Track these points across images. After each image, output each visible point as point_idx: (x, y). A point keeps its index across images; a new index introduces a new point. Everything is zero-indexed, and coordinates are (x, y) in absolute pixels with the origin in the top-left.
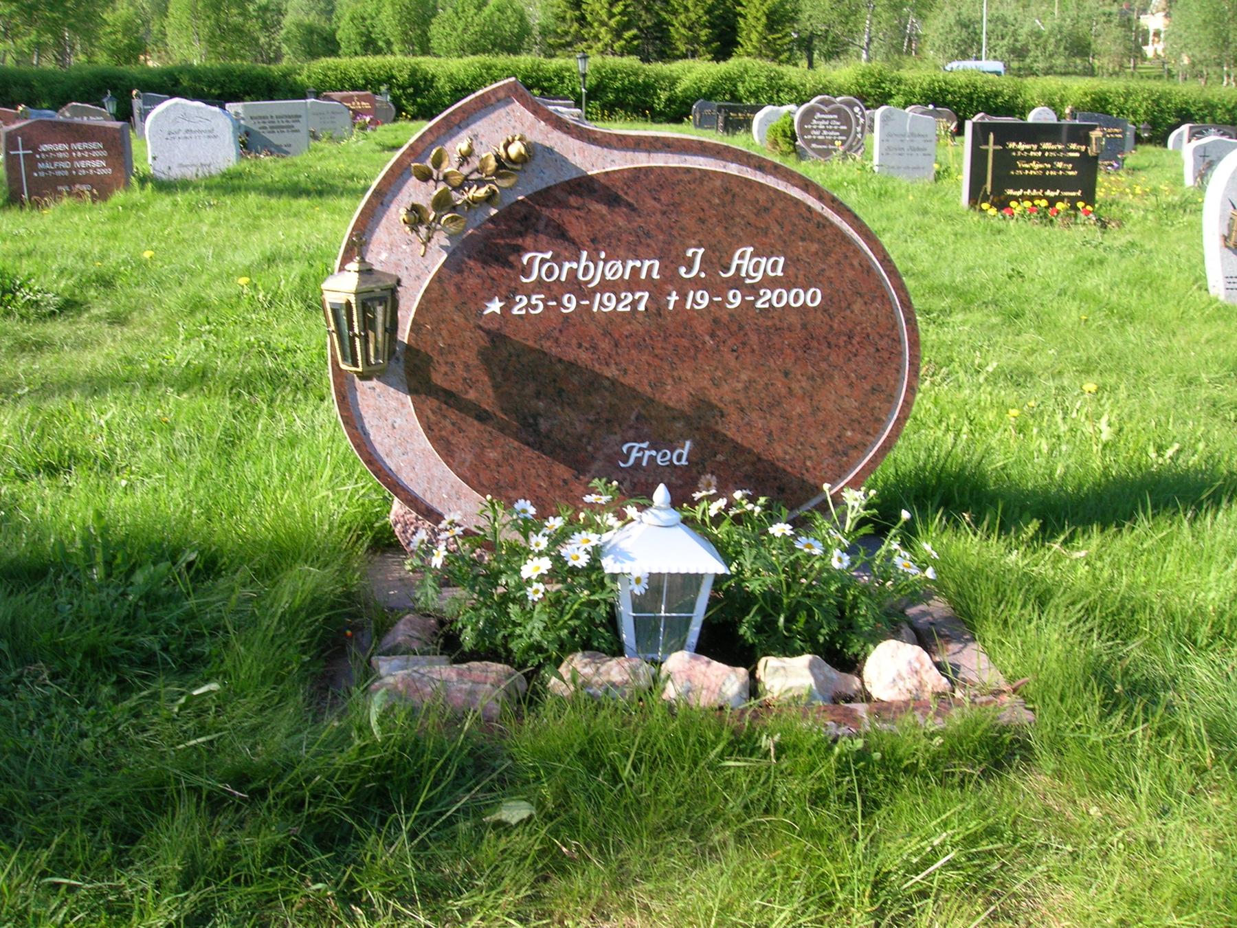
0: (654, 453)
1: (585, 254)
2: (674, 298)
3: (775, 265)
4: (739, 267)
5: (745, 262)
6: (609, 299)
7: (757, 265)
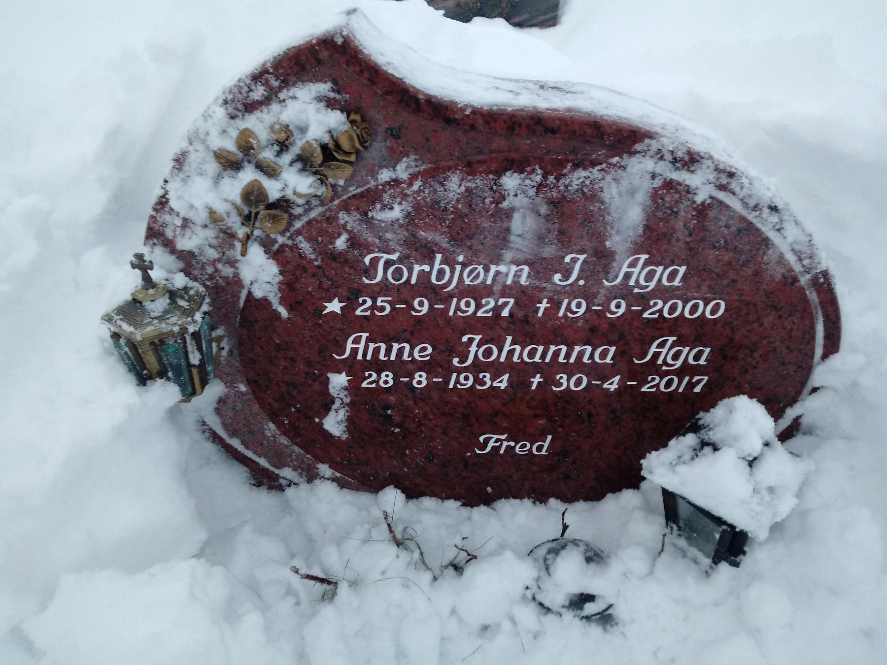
0: (512, 444)
1: (439, 257)
2: (544, 305)
3: (672, 276)
4: (628, 276)
5: (636, 270)
6: (468, 304)
7: (651, 274)
